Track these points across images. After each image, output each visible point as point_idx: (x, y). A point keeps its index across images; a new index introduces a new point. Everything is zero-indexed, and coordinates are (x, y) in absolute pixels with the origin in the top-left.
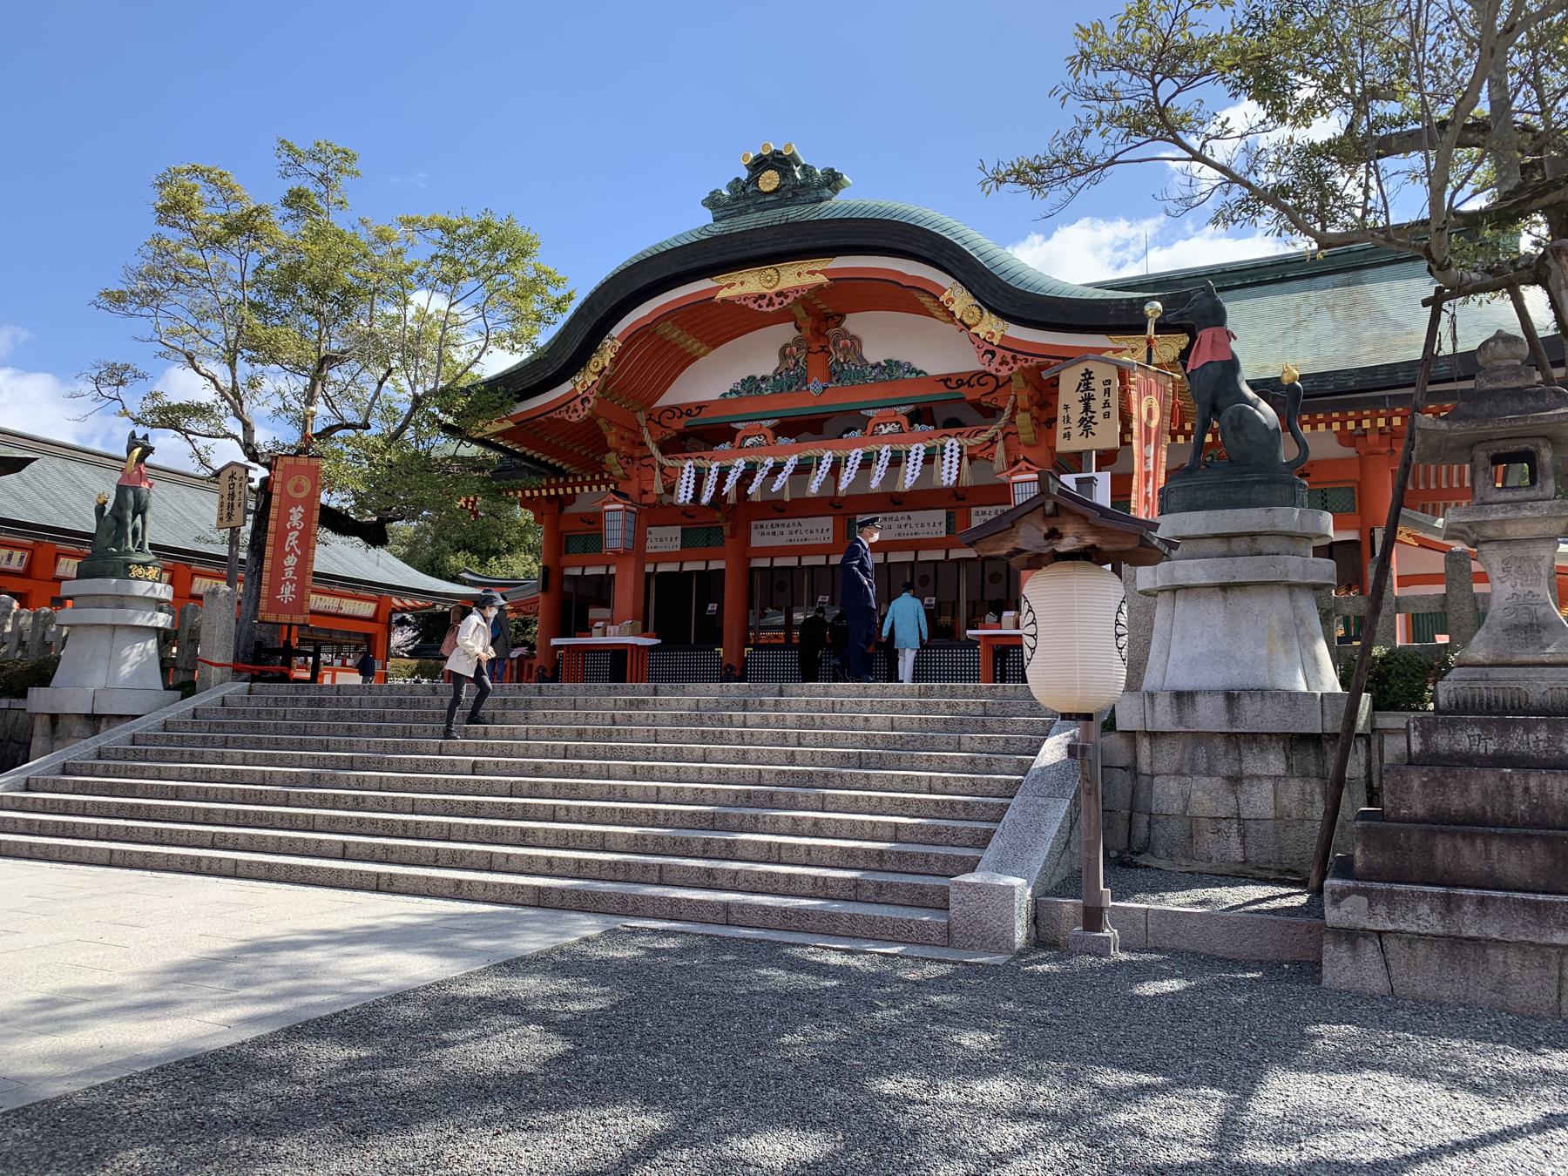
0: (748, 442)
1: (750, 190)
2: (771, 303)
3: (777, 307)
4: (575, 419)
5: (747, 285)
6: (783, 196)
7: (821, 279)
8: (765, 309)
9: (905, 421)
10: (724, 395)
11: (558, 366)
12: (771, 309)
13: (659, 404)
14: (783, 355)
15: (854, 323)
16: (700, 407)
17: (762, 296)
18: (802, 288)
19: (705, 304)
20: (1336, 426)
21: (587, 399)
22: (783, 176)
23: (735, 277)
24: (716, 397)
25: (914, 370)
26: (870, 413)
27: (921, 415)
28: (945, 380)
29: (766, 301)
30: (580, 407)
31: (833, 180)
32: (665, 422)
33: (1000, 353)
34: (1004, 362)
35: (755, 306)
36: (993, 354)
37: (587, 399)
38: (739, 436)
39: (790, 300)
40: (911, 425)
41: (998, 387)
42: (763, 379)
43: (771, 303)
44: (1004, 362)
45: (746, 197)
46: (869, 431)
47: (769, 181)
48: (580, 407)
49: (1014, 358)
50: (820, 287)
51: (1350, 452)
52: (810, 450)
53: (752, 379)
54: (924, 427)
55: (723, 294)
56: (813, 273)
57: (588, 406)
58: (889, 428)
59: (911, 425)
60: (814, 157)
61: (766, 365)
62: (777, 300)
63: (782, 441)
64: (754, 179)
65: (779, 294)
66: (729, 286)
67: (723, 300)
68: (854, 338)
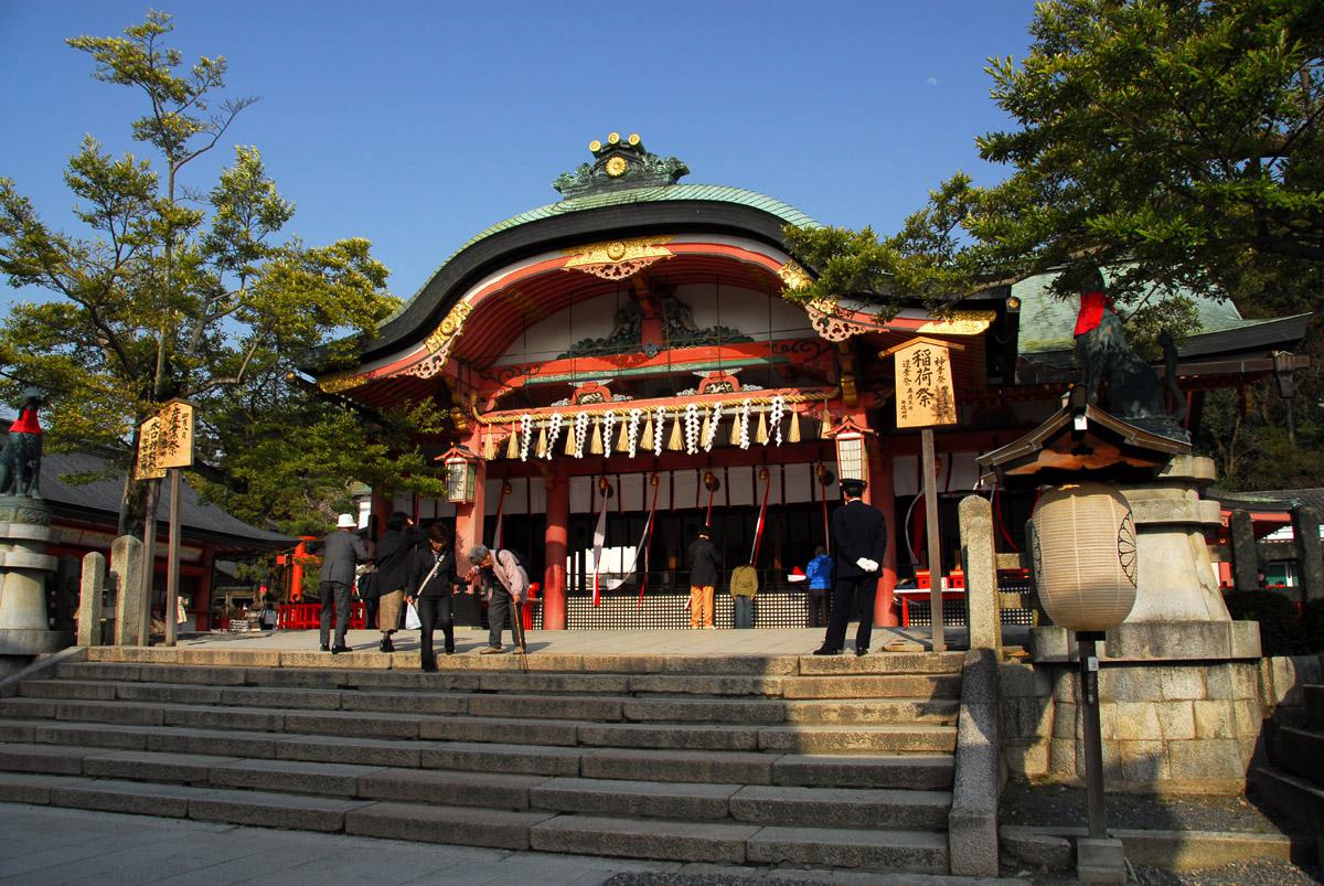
0: (585, 399)
2: (618, 272)
4: (426, 375)
5: (592, 259)
6: (625, 180)
7: (663, 252)
8: (612, 277)
9: (735, 382)
11: (412, 327)
12: (617, 278)
17: (608, 267)
19: (557, 275)
21: (439, 358)
22: (630, 160)
23: (586, 251)
26: (702, 374)
29: (613, 270)
30: (431, 365)
33: (833, 322)
34: (837, 330)
36: (826, 323)
37: (439, 358)
39: (636, 270)
40: (741, 385)
42: (600, 340)
43: (618, 272)
44: (837, 330)
45: (594, 179)
46: (701, 390)
47: (616, 166)
48: (431, 365)
49: (846, 326)
50: (664, 260)
53: (589, 340)
57: (439, 364)
59: (741, 385)
61: (603, 332)
63: (617, 397)
64: (602, 165)
65: (627, 264)
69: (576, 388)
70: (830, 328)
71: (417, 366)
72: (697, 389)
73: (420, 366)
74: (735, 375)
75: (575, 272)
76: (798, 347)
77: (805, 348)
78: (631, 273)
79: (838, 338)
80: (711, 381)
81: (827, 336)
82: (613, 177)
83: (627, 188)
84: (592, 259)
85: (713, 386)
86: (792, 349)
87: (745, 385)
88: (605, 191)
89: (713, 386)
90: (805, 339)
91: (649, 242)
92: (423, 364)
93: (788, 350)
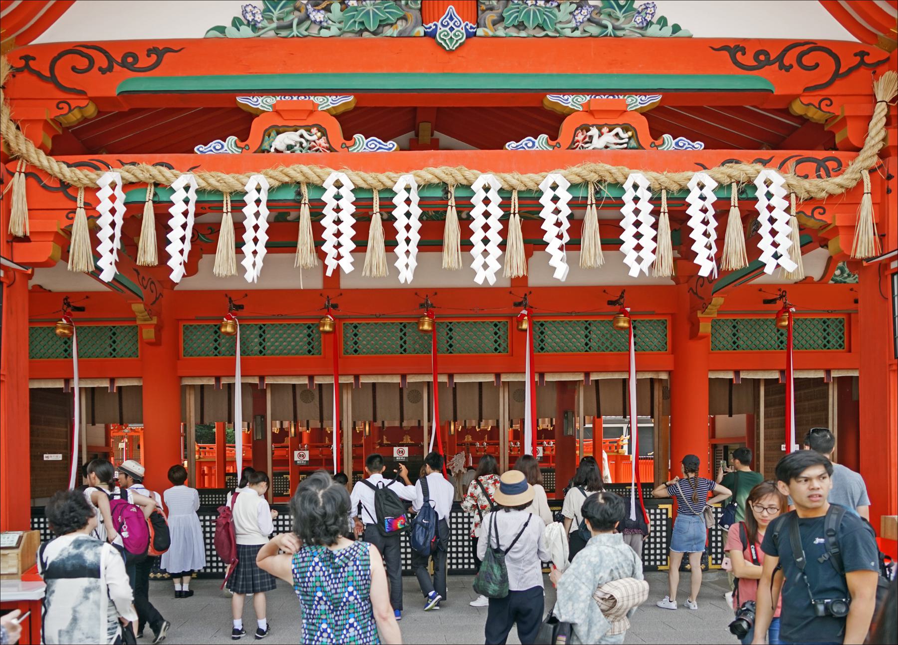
0: (281, 141)
9: (642, 125)
10: (221, 29)
13: (44, 38)
16: (160, 52)
24: (197, 31)
25: (663, 21)
28: (733, 49)
38: (257, 127)
40: (656, 134)
41: (837, 75)
52: (444, 168)
54: (683, 141)
58: (609, 138)
59: (656, 134)
63: (362, 143)
72: (553, 137)
74: (645, 113)
76: (790, 58)
77: (806, 60)
80: (590, 120)
85: (594, 131)
86: (781, 58)
87: (667, 137)
89: (594, 131)
90: (806, 42)
93: (769, 62)
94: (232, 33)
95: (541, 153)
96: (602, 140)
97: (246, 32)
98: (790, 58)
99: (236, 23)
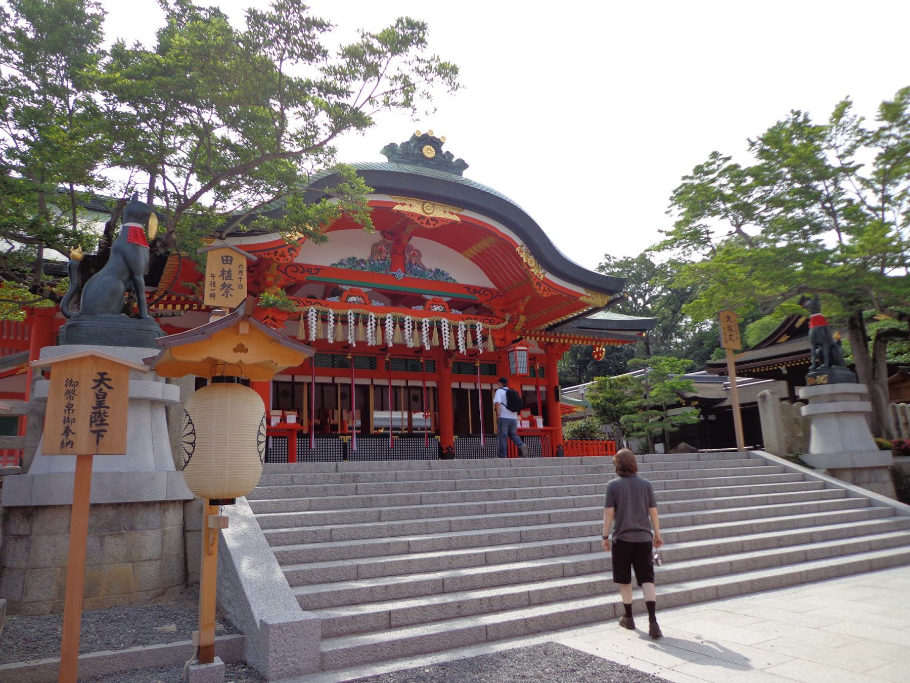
0: (351, 299)
1: (416, 152)
2: (428, 223)
3: (431, 226)
5: (414, 208)
7: (457, 219)
8: (424, 225)
12: (428, 226)
14: (376, 249)
15: (417, 242)
16: (318, 269)
18: (447, 220)
20: (538, 339)
23: (408, 202)
26: (428, 297)
27: (452, 304)
28: (468, 288)
31: (462, 165)
32: (289, 271)
35: (419, 222)
42: (362, 261)
43: (428, 223)
45: (413, 155)
46: (427, 307)
50: (454, 223)
51: (542, 352)
53: (354, 258)
55: (397, 208)
56: (453, 214)
58: (438, 308)
60: (453, 147)
61: (364, 254)
62: (432, 223)
63: (375, 303)
65: (433, 219)
66: (403, 204)
67: (398, 211)
68: (417, 251)
69: (345, 290)
70: (542, 288)
71: (272, 252)
73: (276, 253)
75: (399, 213)
76: (482, 292)
78: (438, 225)
79: (545, 295)
81: (540, 292)
82: (427, 158)
83: (438, 169)
84: (414, 208)
88: (424, 166)
91: (447, 210)
92: (280, 251)
94: (339, 267)
95: (420, 311)
96: (436, 308)
97: (343, 267)
98: (482, 292)
99: (341, 263)
